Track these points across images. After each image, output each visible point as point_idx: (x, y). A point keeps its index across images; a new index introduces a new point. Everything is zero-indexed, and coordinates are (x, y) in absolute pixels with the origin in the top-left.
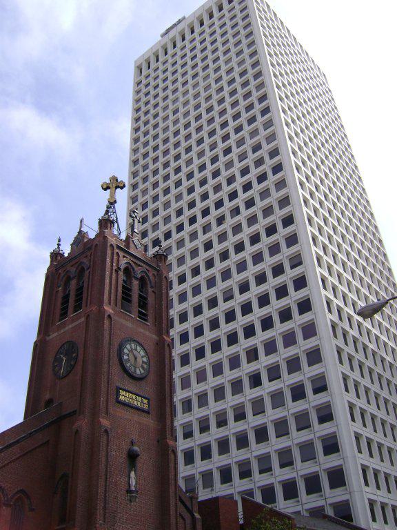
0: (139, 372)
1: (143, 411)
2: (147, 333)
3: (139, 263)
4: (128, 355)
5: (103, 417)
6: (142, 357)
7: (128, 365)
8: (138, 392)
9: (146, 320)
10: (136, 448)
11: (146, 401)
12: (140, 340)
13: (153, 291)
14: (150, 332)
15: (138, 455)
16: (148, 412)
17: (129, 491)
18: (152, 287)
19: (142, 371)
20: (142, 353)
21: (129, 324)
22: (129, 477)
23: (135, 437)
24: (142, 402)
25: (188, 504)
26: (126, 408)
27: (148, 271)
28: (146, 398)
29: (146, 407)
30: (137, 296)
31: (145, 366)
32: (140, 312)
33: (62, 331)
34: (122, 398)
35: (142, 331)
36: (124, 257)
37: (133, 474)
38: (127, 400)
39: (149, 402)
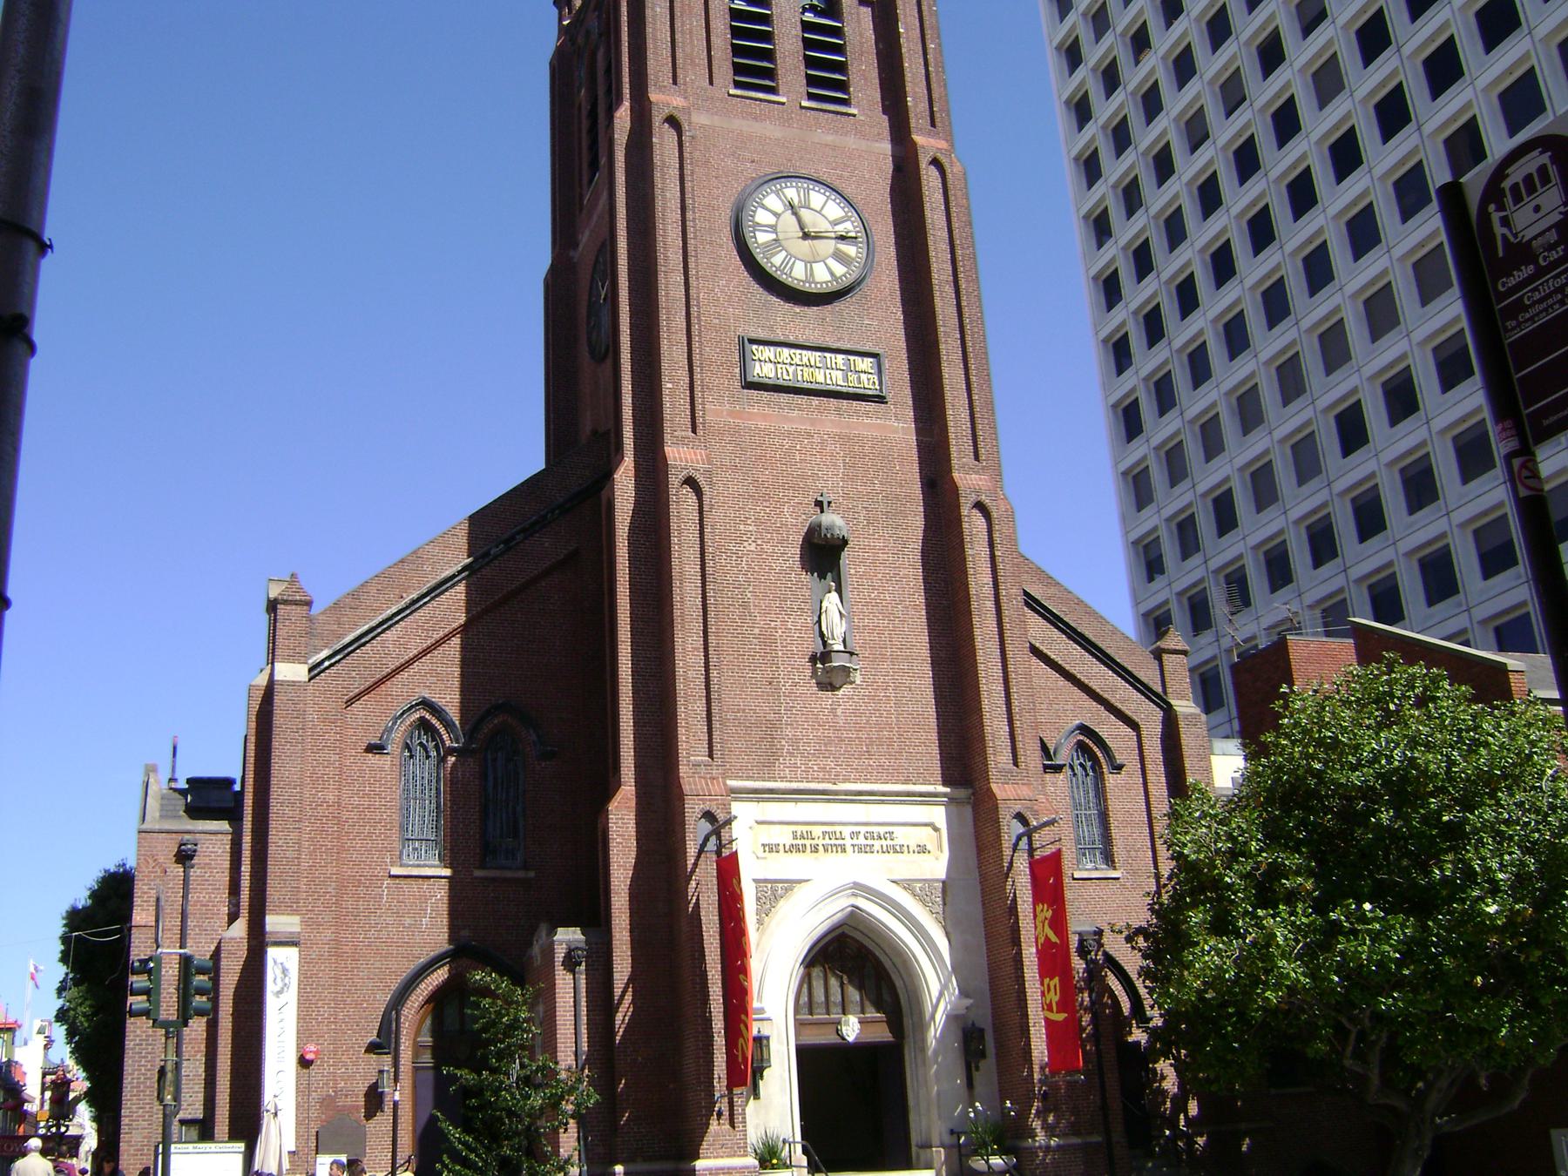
0: (823, 275)
2: (851, 142)
4: (774, 229)
5: (682, 441)
6: (835, 223)
7: (778, 260)
9: (845, 102)
10: (833, 520)
11: (865, 364)
14: (864, 136)
15: (844, 542)
16: (880, 399)
19: (840, 270)
20: (835, 210)
21: (770, 130)
23: (831, 484)
24: (849, 369)
25: (1149, 675)
26: (784, 398)
29: (869, 383)
30: (798, 31)
32: (811, 81)
33: (595, 218)
35: (829, 138)
38: (787, 376)
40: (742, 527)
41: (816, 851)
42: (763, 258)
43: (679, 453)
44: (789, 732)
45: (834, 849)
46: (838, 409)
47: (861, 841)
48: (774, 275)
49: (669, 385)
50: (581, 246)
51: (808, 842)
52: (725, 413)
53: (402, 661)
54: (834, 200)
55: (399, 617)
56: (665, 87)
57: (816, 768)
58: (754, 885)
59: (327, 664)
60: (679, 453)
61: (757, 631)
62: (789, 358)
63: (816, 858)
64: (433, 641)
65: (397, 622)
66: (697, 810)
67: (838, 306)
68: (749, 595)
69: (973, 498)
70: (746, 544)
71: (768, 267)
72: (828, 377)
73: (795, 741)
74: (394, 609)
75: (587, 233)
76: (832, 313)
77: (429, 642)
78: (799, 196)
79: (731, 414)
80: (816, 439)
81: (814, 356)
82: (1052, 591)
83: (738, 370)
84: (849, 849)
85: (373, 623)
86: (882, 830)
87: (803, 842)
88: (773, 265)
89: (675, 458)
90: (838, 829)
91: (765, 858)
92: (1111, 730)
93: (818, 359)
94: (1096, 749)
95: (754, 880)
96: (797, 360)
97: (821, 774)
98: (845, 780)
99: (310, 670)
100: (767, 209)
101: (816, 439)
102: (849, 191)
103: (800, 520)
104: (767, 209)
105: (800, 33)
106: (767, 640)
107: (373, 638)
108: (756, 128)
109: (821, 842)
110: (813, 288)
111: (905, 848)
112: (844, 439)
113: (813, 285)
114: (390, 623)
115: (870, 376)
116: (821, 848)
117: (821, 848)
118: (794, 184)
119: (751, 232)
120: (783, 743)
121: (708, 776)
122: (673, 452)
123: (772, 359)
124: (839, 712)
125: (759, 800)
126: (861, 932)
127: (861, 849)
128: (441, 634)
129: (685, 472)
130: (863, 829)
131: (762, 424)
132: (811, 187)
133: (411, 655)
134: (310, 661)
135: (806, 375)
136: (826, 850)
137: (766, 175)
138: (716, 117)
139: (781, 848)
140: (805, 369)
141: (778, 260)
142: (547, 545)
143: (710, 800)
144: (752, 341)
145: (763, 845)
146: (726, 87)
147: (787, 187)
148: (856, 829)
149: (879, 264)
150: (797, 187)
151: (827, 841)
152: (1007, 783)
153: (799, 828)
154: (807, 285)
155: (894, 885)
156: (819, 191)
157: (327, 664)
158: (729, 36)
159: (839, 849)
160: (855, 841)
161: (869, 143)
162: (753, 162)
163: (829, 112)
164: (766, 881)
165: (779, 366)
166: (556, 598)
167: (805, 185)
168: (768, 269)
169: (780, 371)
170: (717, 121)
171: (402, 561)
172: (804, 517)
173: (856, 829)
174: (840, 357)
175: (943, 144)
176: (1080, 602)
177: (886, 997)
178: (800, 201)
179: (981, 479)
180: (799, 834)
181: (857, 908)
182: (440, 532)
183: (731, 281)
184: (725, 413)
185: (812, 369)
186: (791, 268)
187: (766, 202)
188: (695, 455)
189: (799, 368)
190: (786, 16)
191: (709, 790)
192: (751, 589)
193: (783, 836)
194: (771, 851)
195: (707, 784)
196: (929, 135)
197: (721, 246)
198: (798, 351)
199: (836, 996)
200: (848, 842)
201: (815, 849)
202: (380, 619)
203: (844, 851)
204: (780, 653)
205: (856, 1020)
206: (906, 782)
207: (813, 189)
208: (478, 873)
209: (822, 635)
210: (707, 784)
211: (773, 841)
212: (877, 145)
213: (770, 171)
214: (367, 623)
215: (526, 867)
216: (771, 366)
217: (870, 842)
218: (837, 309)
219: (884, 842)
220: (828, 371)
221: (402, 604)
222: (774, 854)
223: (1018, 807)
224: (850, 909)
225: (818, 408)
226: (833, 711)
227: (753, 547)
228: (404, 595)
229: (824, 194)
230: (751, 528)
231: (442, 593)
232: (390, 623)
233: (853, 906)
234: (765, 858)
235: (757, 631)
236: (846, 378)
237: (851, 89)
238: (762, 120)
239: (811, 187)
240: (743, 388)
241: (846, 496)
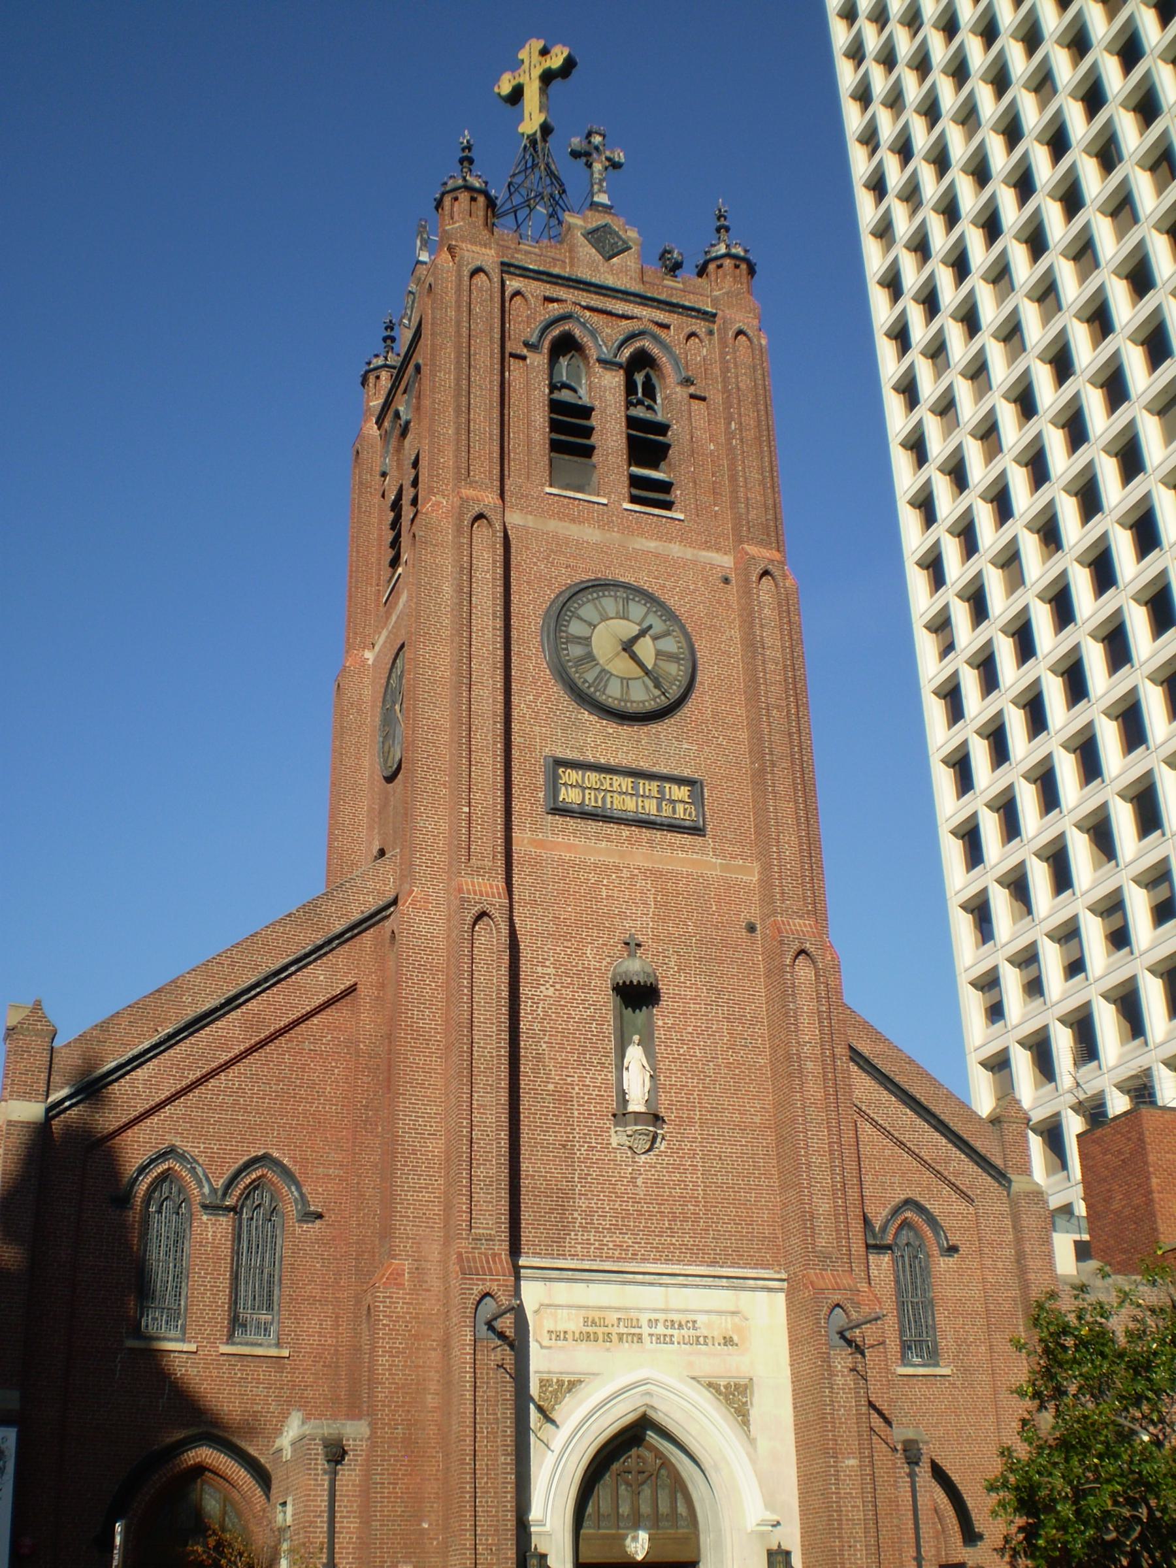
1: (673, 827)
2: (676, 550)
3: (620, 307)
8: (644, 765)
9: (668, 505)
11: (682, 793)
12: (644, 580)
13: (692, 396)
16: (697, 830)
17: (621, 1116)
18: (688, 382)
21: (590, 534)
22: (620, 1067)
23: (641, 924)
26: (592, 826)
27: (666, 327)
28: (681, 781)
31: (672, 669)
33: (394, 618)
34: (570, 796)
36: (549, 300)
37: (635, 1054)
38: (591, 801)
39: (697, 798)
40: (539, 969)
42: (577, 672)
43: (473, 885)
44: (582, 1203)
45: (630, 1338)
46: (650, 841)
47: (660, 1330)
48: (586, 691)
49: (466, 809)
50: (377, 648)
51: (600, 1331)
52: (526, 841)
53: (152, 1103)
54: (656, 612)
55: (151, 1054)
56: (477, 482)
57: (611, 1245)
59: (67, 1104)
60: (473, 885)
61: (551, 1087)
62: (599, 783)
63: (608, 1350)
64: (188, 1082)
65: (150, 1059)
66: (475, 1292)
67: (654, 728)
68: (544, 1046)
69: (796, 946)
70: (542, 988)
71: (579, 683)
72: (640, 804)
73: (589, 1213)
74: (146, 1045)
75: (385, 633)
76: (648, 735)
77: (184, 1083)
78: (617, 607)
79: (533, 842)
80: (625, 873)
81: (626, 783)
82: (879, 1048)
83: (541, 795)
84: (646, 1338)
85: (122, 1060)
87: (595, 1329)
88: (585, 681)
89: (468, 890)
91: (549, 1348)
92: (945, 1204)
93: (630, 785)
94: (926, 1228)
96: (606, 786)
97: (617, 1253)
98: (644, 1260)
99: (49, 1110)
100: (581, 619)
101: (625, 873)
102: (671, 603)
103: (604, 963)
104: (581, 619)
105: (624, 429)
106: (563, 1098)
107: (122, 1076)
108: (574, 531)
109: (615, 1330)
110: (631, 708)
111: (709, 1341)
112: (656, 875)
113: (629, 705)
114: (142, 1059)
115: (687, 806)
116: (615, 1338)
117: (615, 1338)
118: (612, 593)
119: (563, 643)
120: (576, 1215)
121: (490, 1252)
122: (467, 884)
123: (580, 781)
124: (639, 1182)
127: (662, 1339)
128: (198, 1074)
129: (479, 907)
131: (567, 856)
132: (631, 597)
133: (163, 1097)
134: (50, 1100)
135: (615, 802)
136: (621, 1340)
137: (583, 582)
138: (530, 517)
140: (615, 795)
141: (590, 676)
142: (322, 978)
143: (491, 1280)
144: (560, 763)
146: (543, 485)
147: (604, 596)
149: (702, 684)
150: (616, 597)
151: (623, 1330)
152: (826, 1270)
154: (623, 704)
155: (694, 1383)
156: (639, 602)
157: (67, 1104)
158: (547, 430)
159: (635, 1339)
160: (653, 1331)
161: (695, 552)
162: (567, 567)
163: (654, 515)
165: (587, 791)
166: (329, 1038)
167: (625, 595)
168: (580, 684)
169: (587, 797)
170: (530, 521)
171: (157, 991)
172: (608, 960)
173: (654, 1316)
174: (654, 786)
175: (776, 556)
176: (911, 1062)
177: (682, 1509)
178: (618, 613)
179: (805, 925)
180: (590, 1320)
181: (652, 1407)
182: (203, 960)
183: (537, 696)
184: (526, 841)
185: (624, 796)
186: (605, 686)
187: (582, 612)
188: (491, 887)
189: (609, 795)
190: (610, 410)
191: (490, 1269)
192: (546, 1040)
193: (572, 1323)
195: (488, 1262)
196: (761, 543)
197: (530, 658)
198: (608, 777)
199: (625, 1509)
200: (645, 1330)
201: (608, 1337)
202: (130, 1055)
204: (576, 1113)
205: (646, 1536)
206: (713, 1263)
207: (633, 600)
208: (225, 1349)
209: (624, 1093)
210: (488, 1262)
211: (561, 1327)
212: (704, 553)
213: (585, 577)
214: (115, 1059)
215: (278, 1345)
216: (577, 790)
217: (669, 1332)
218: (654, 730)
219: (684, 1332)
220: (640, 799)
221: (155, 1039)
222: (560, 1343)
223: (837, 1297)
224: (643, 1409)
225: (628, 839)
226: (633, 1180)
227: (551, 992)
228: (159, 1029)
229: (645, 605)
230: (551, 971)
231: (202, 1028)
232: (142, 1059)
233: (647, 1405)
234: (549, 1348)
235: (551, 1087)
236: (659, 809)
237: (678, 492)
238: (580, 522)
239: (631, 597)
240: (548, 813)
241: (656, 939)
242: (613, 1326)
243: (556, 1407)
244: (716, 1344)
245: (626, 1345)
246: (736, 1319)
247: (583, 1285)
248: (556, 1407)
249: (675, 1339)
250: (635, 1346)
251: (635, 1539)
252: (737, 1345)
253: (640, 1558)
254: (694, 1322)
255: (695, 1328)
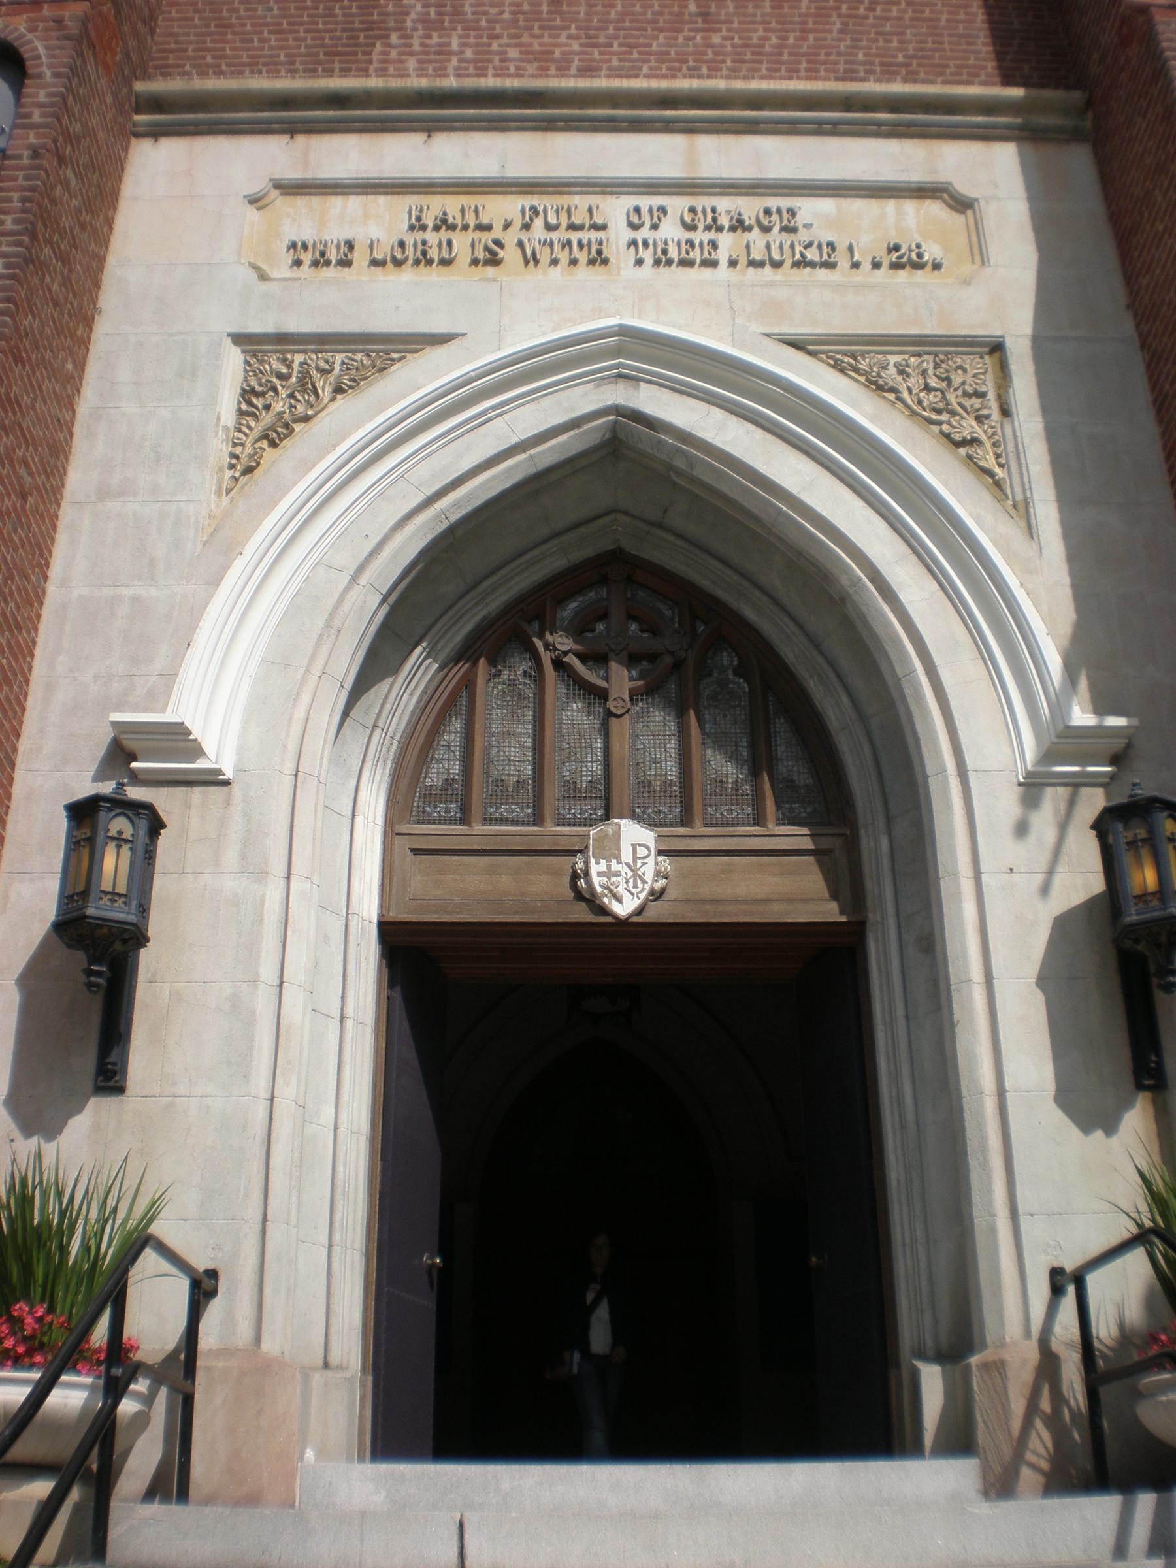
41: (494, 261)
58: (234, 359)
86: (749, 208)
90: (580, 202)
95: (239, 339)
111: (844, 263)
116: (510, 254)
125: (292, 129)
126: (680, 536)
130: (677, 205)
139: (360, 257)
145: (293, 245)
148: (646, 202)
153: (436, 205)
160: (645, 233)
164: (283, 340)
181: (637, 417)
194: (320, 261)
200: (619, 233)
203: (599, 259)
211: (336, 233)
222: (331, 272)
233: (617, 410)
242: (507, 226)
243: (297, 427)
244: (866, 265)
245: (556, 273)
246: (936, 209)
247: (418, 138)
248: (297, 427)
249: (722, 256)
250: (583, 273)
251: (610, 848)
252: (937, 266)
253: (623, 908)
254: (792, 212)
255: (789, 230)
